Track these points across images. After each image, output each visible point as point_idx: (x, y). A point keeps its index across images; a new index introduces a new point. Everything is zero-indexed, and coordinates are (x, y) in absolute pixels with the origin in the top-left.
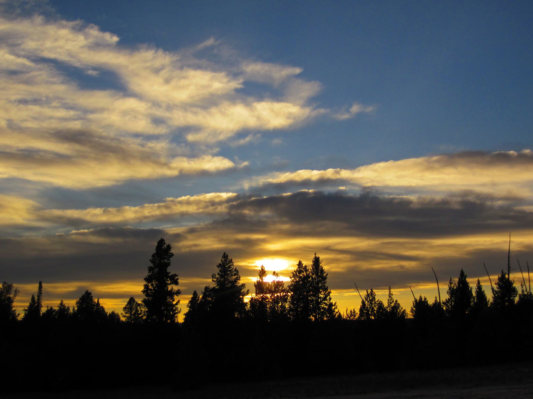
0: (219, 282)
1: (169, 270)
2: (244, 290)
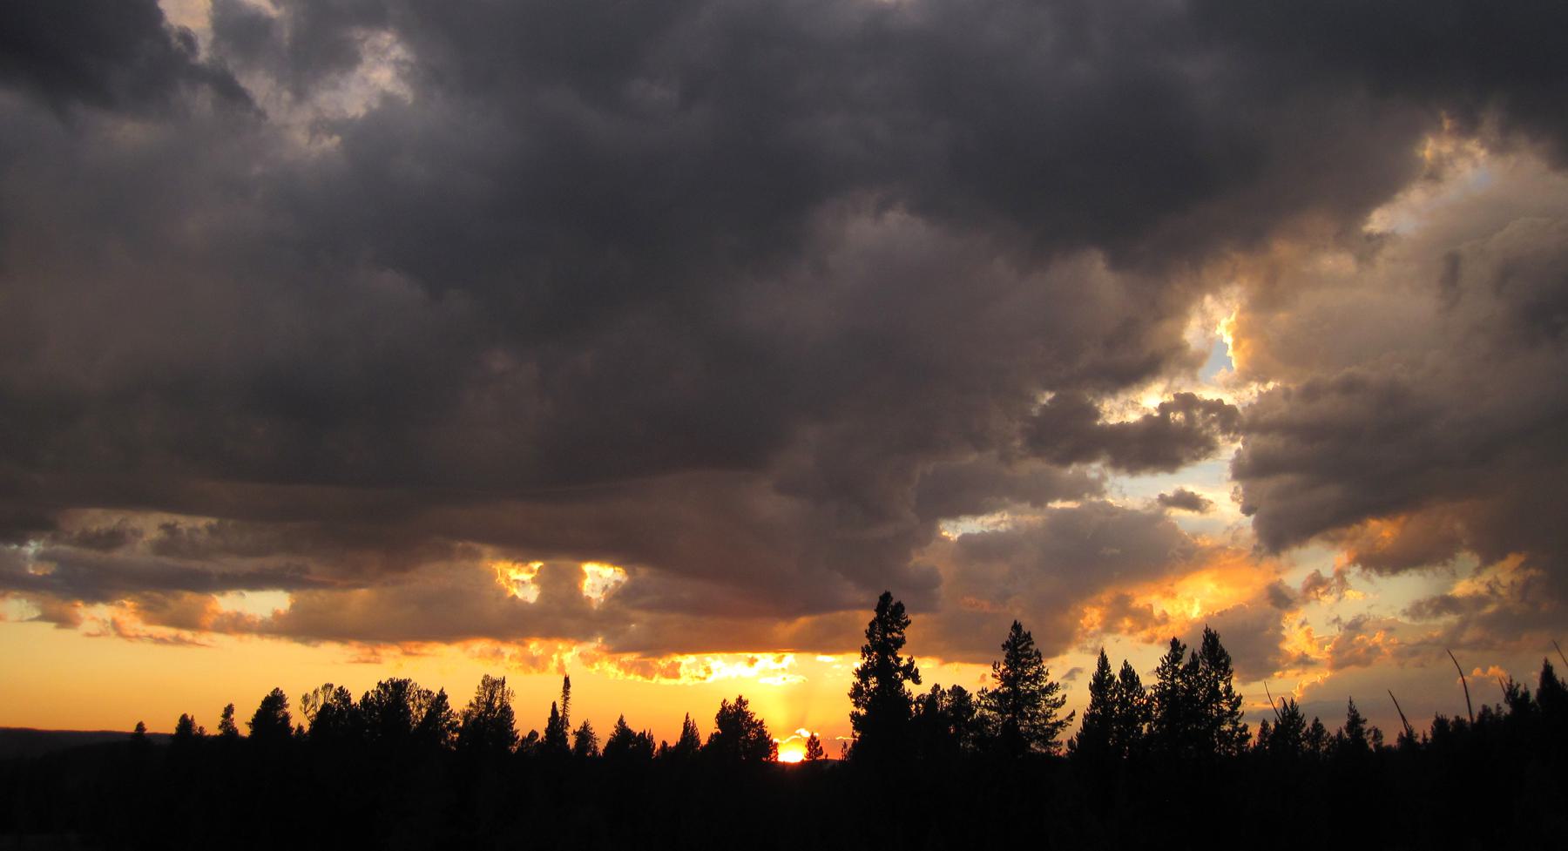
0: (1006, 680)
2: (1058, 695)
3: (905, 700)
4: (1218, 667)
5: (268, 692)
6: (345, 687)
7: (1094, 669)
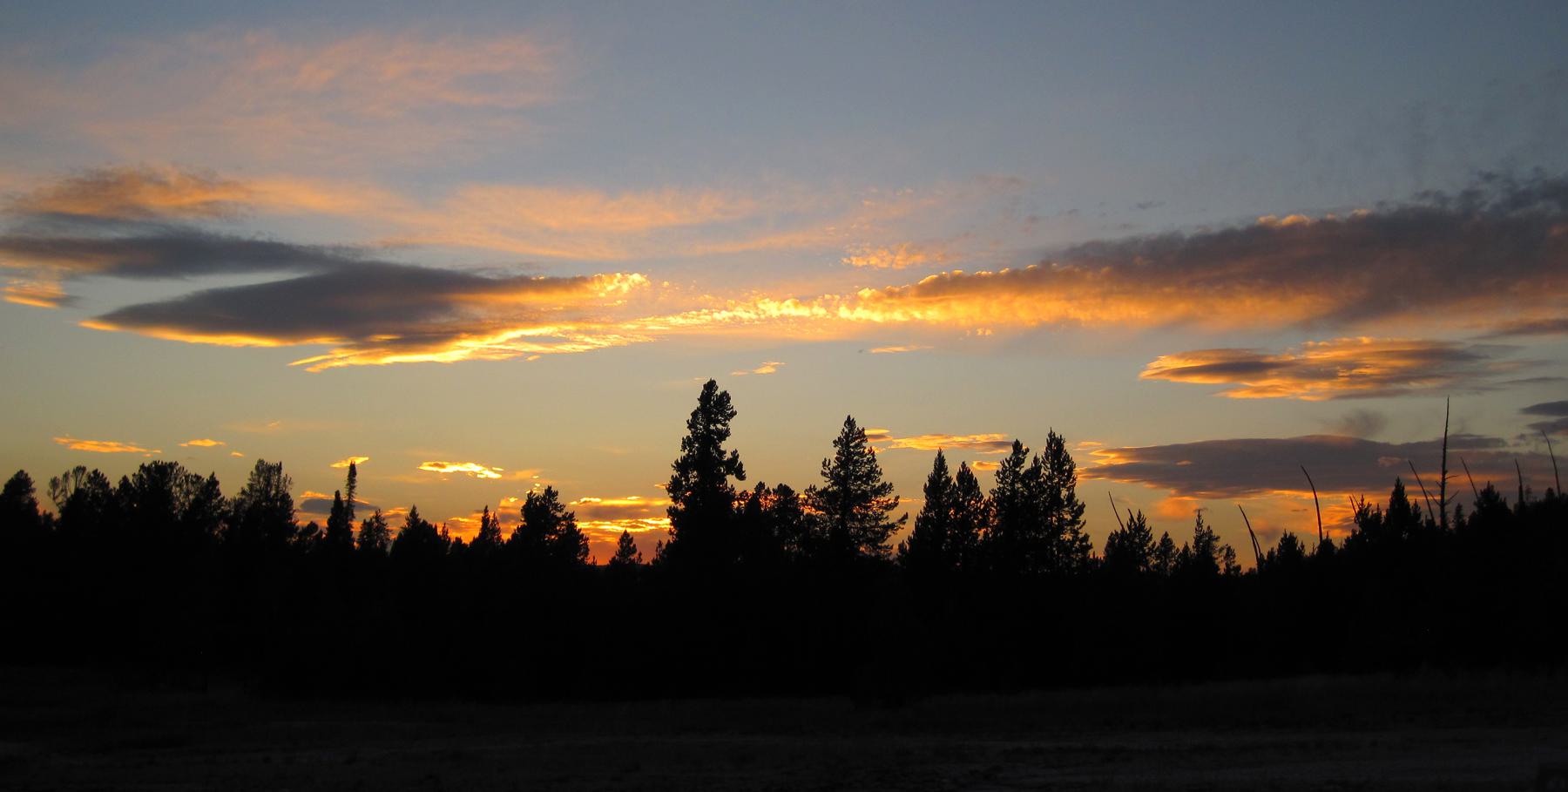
0: (834, 477)
1: (724, 446)
3: (730, 496)
4: (1062, 472)
5: (10, 474)
6: (101, 471)
7: (931, 470)
